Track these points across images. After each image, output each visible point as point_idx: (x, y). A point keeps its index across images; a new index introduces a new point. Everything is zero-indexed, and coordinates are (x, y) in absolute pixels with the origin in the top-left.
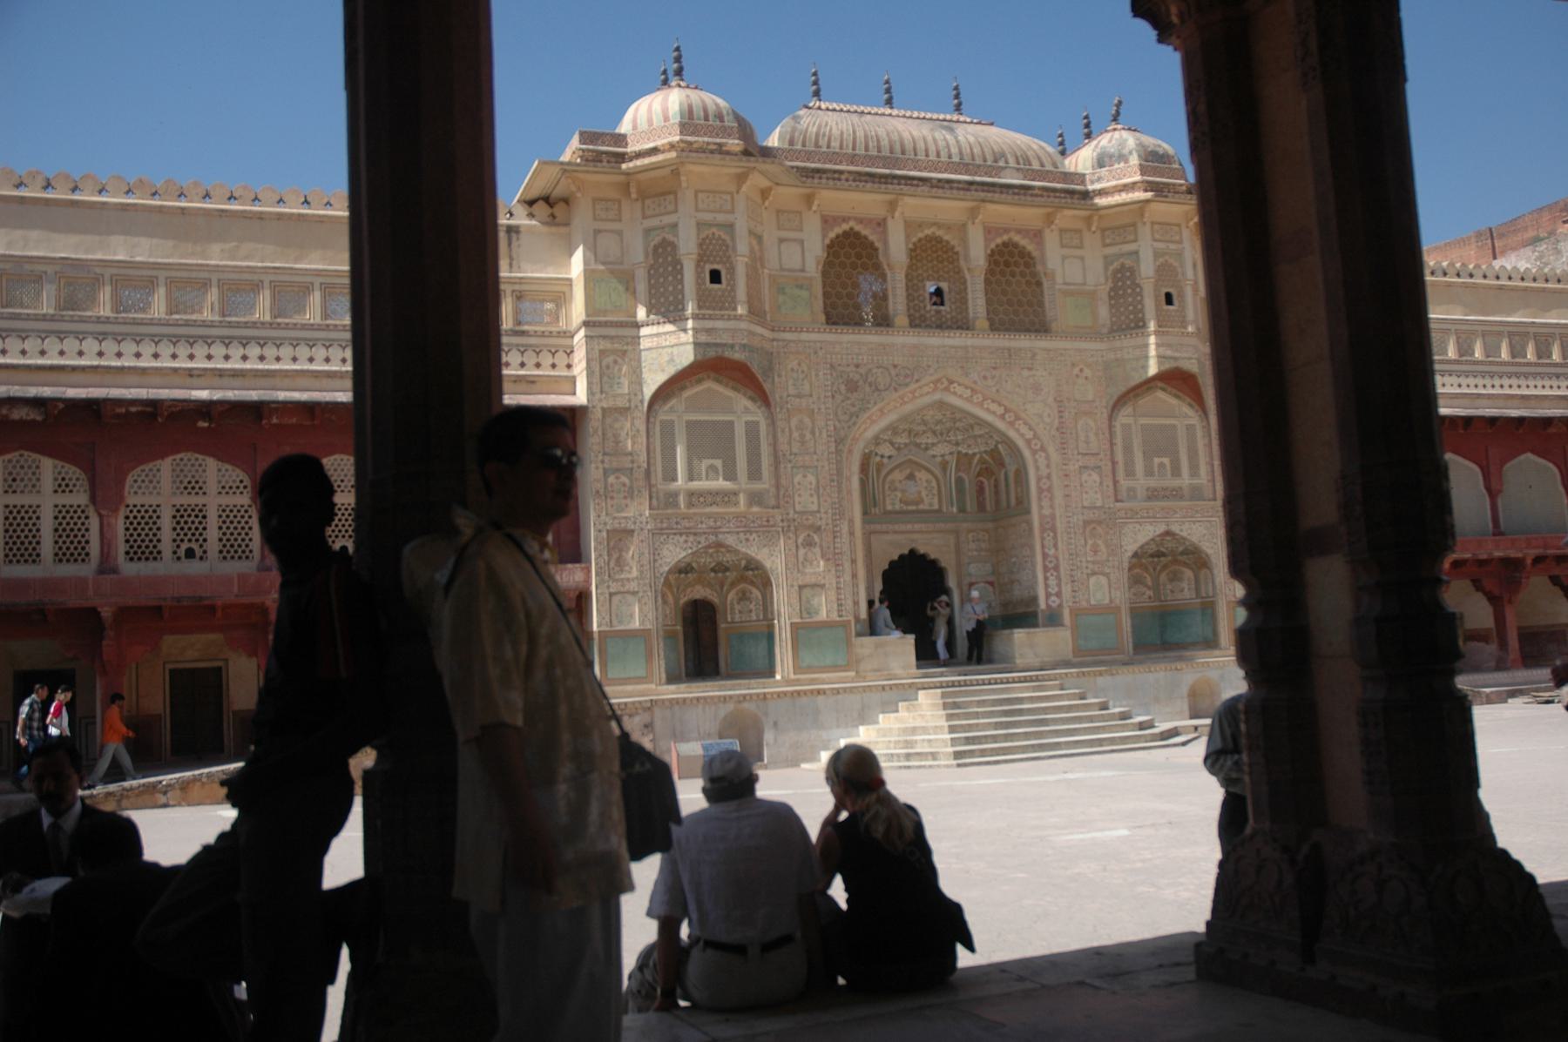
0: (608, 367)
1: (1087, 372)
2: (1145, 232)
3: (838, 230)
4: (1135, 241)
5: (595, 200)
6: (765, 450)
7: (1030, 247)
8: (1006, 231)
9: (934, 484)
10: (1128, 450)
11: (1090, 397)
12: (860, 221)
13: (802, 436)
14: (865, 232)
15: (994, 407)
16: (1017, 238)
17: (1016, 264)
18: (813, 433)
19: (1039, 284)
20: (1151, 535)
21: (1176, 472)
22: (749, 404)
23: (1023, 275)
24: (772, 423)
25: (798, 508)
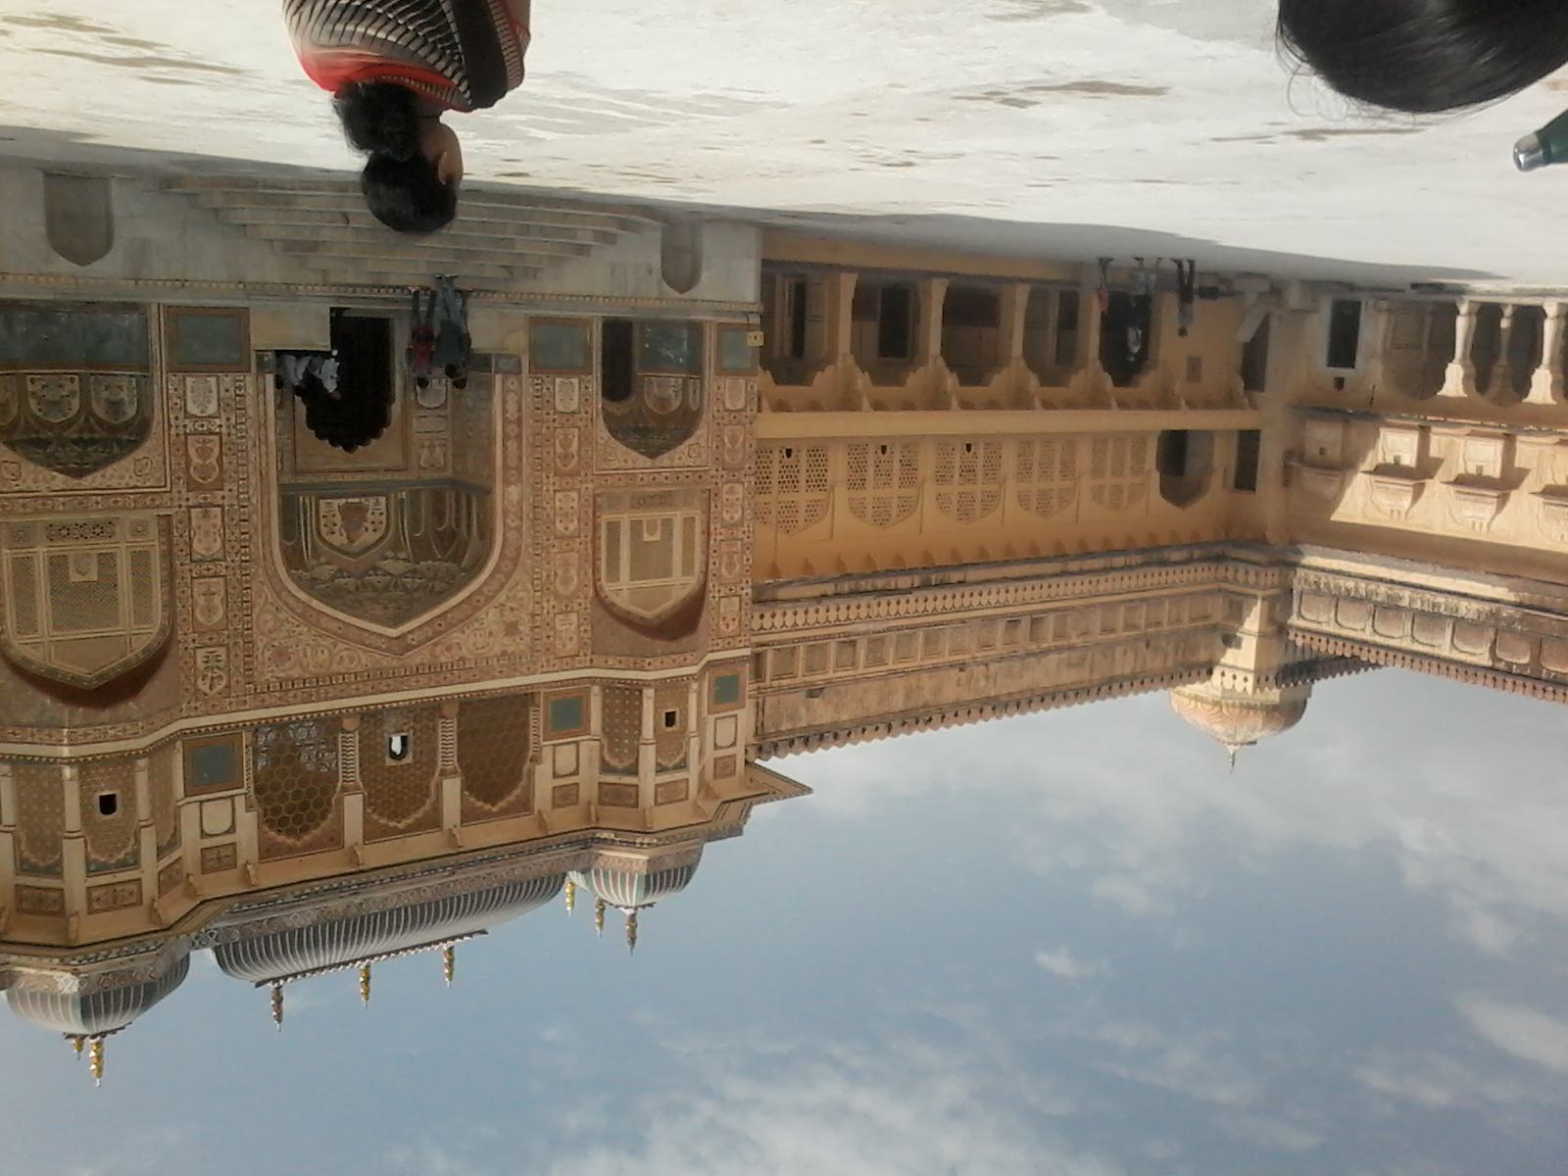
0: (734, 619)
1: (207, 690)
2: (149, 888)
3: (511, 798)
4: (160, 873)
5: (733, 773)
6: (603, 555)
7: (272, 834)
8: (310, 848)
9: (324, 530)
10: (141, 587)
11: (201, 653)
12: (487, 816)
13: (566, 571)
14: (480, 804)
15: (333, 626)
16: (290, 841)
17: (291, 809)
18: (556, 573)
19: (258, 791)
20: (109, 471)
21: (57, 565)
22: (618, 601)
23: (284, 797)
24: (596, 580)
25: (574, 495)
